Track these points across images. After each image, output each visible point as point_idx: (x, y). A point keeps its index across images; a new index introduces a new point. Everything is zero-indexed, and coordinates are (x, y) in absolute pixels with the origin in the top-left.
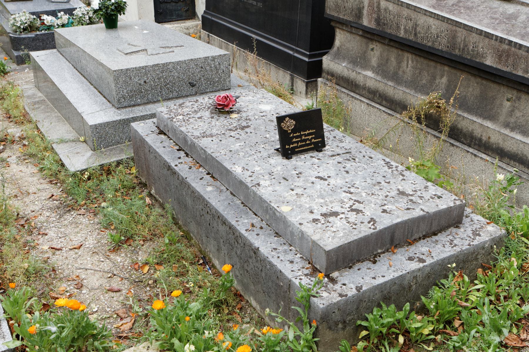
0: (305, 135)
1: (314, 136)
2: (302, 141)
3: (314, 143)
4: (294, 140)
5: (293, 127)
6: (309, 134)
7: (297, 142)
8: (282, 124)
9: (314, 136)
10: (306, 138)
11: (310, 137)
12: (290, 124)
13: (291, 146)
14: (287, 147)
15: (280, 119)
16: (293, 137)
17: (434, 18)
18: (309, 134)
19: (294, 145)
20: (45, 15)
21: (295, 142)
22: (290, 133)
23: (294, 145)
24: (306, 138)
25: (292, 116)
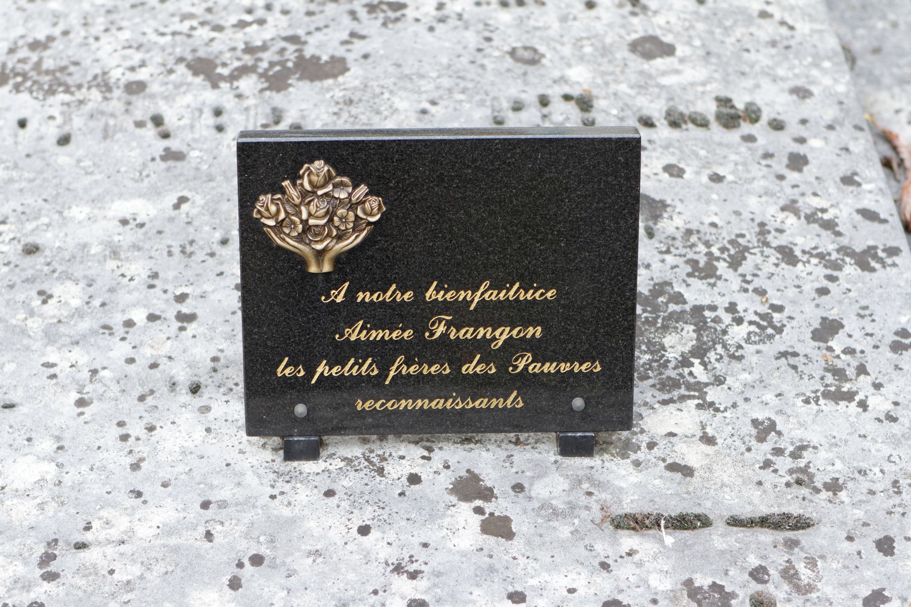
0: (461, 315)
1: (535, 332)
2: (418, 350)
3: (525, 381)
4: (355, 333)
5: (352, 241)
6: (490, 314)
7: (383, 353)
8: (265, 199)
9: (535, 332)
10: (466, 333)
11: (503, 335)
12: (327, 219)
13: (322, 369)
14: (284, 370)
15: (265, 164)
16: (351, 312)
17: (264, 395)
18: (490, 314)
19: (350, 369)
20: (639, 289)
21: (359, 350)
22: (330, 281)
23: (350, 369)
24: (466, 333)
25: (354, 157)
